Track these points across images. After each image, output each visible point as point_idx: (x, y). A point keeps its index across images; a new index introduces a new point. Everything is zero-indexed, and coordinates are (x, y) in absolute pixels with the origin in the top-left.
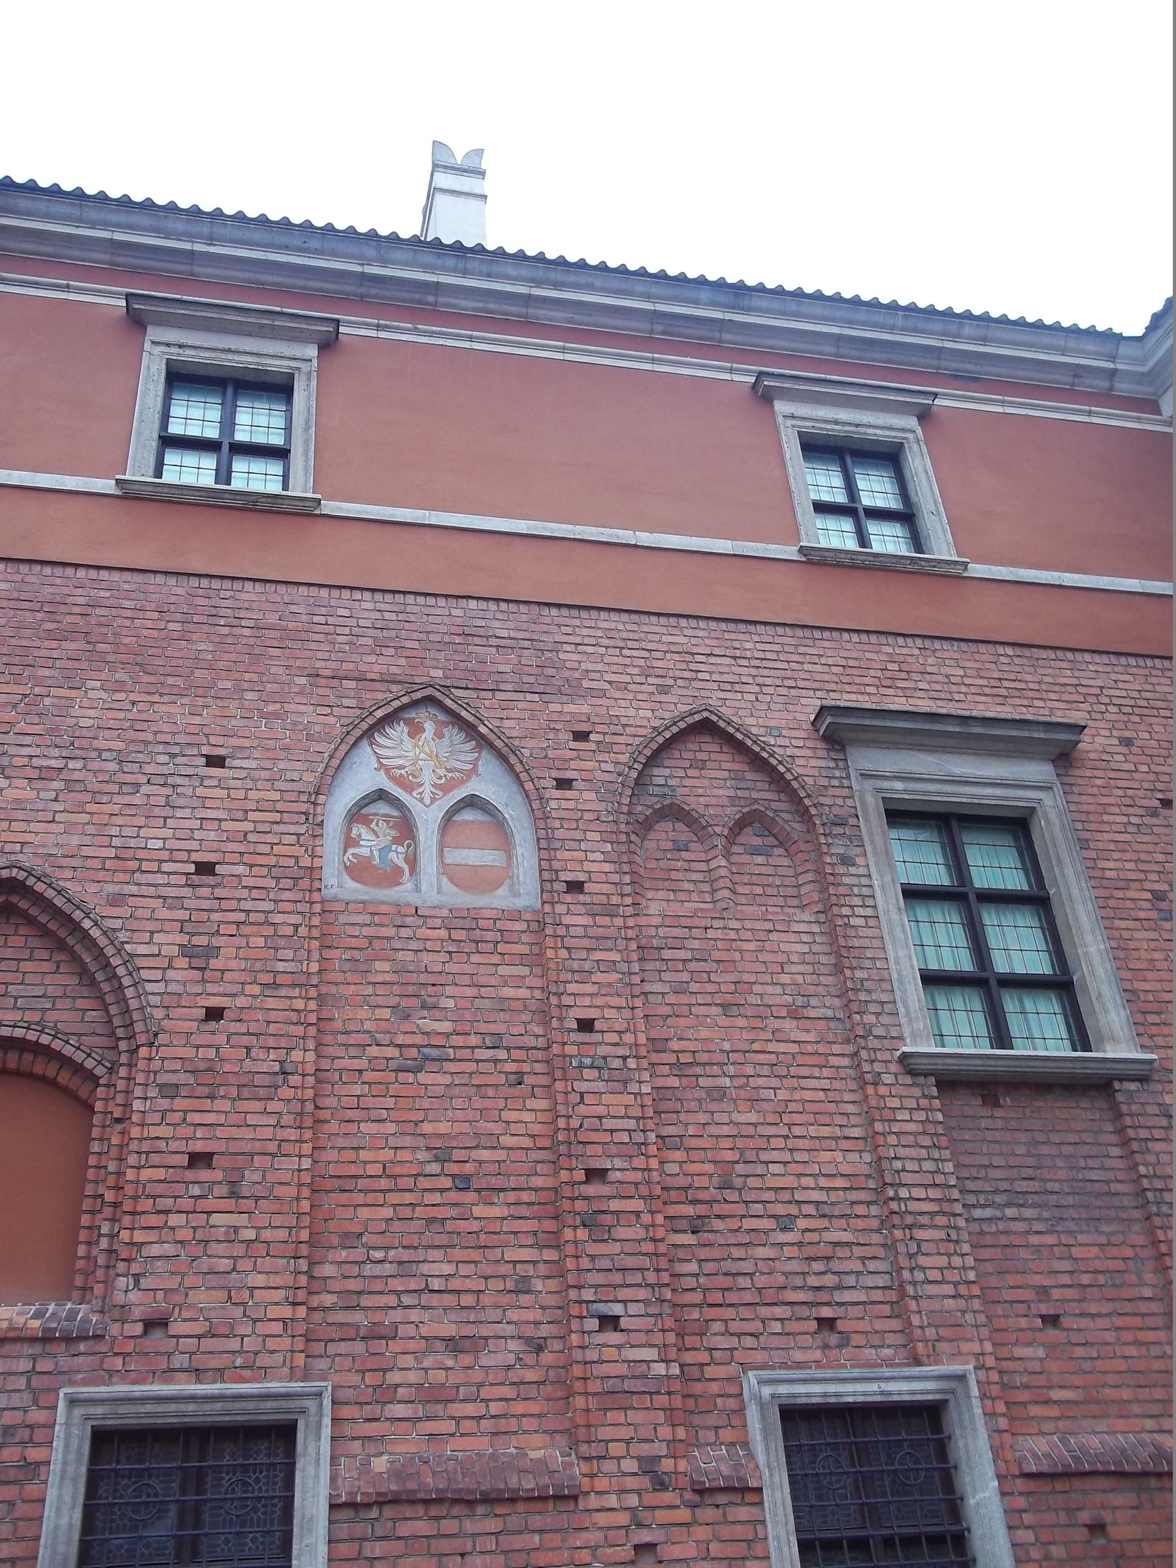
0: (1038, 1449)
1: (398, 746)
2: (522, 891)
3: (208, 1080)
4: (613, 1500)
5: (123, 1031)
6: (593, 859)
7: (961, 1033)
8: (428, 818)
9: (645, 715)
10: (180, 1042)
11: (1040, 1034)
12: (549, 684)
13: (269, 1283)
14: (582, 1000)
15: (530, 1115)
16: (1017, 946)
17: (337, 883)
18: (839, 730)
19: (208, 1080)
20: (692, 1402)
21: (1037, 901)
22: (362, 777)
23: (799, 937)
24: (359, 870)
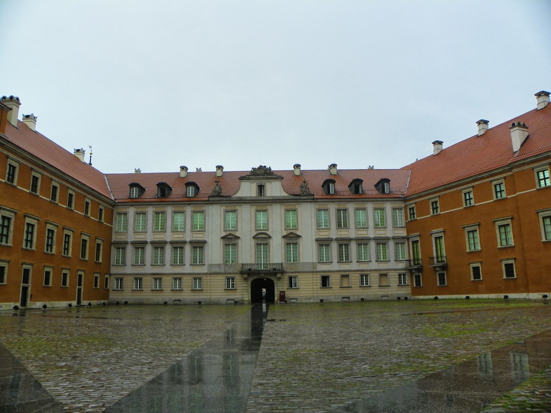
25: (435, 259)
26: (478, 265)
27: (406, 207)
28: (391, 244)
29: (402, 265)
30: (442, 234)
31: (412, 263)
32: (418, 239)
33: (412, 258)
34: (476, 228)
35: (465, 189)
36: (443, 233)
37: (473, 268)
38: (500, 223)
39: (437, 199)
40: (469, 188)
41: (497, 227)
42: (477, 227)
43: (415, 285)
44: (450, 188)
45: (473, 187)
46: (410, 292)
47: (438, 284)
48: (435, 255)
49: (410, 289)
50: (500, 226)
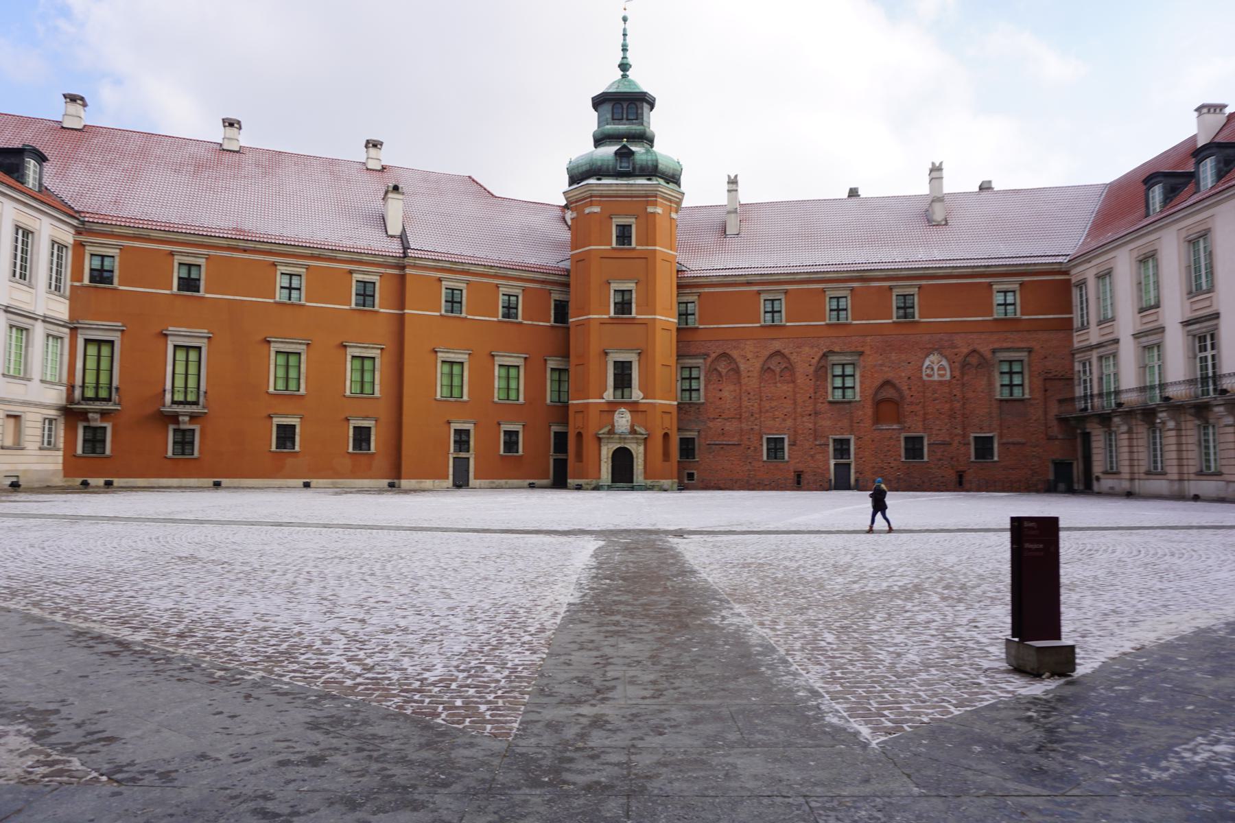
0: (1004, 440)
1: (932, 357)
2: (948, 377)
3: (912, 404)
4: (955, 443)
5: (902, 397)
6: (957, 373)
7: (1006, 394)
8: (936, 368)
9: (965, 351)
10: (909, 399)
11: (1017, 393)
12: (953, 346)
13: (920, 424)
14: (955, 392)
15: (947, 406)
16: (1017, 380)
17: (925, 378)
18: (994, 351)
19: (912, 404)
20: (965, 436)
21: (1021, 373)
22: (927, 363)
23: (984, 382)
24: (928, 375)
25: (168, 397)
26: (294, 421)
27: (79, 246)
28: (39, 330)
29: (55, 396)
30: (203, 343)
31: (77, 393)
32: (115, 337)
33: (78, 381)
34: (301, 348)
35: (287, 264)
36: (206, 341)
37: (279, 426)
38: (357, 352)
39: (202, 261)
40: (301, 266)
41: (349, 358)
42: (304, 347)
43: (79, 451)
44: (245, 251)
45: (308, 268)
46: (60, 467)
47: (170, 453)
48: (168, 386)
49: (60, 460)
50: (353, 357)
